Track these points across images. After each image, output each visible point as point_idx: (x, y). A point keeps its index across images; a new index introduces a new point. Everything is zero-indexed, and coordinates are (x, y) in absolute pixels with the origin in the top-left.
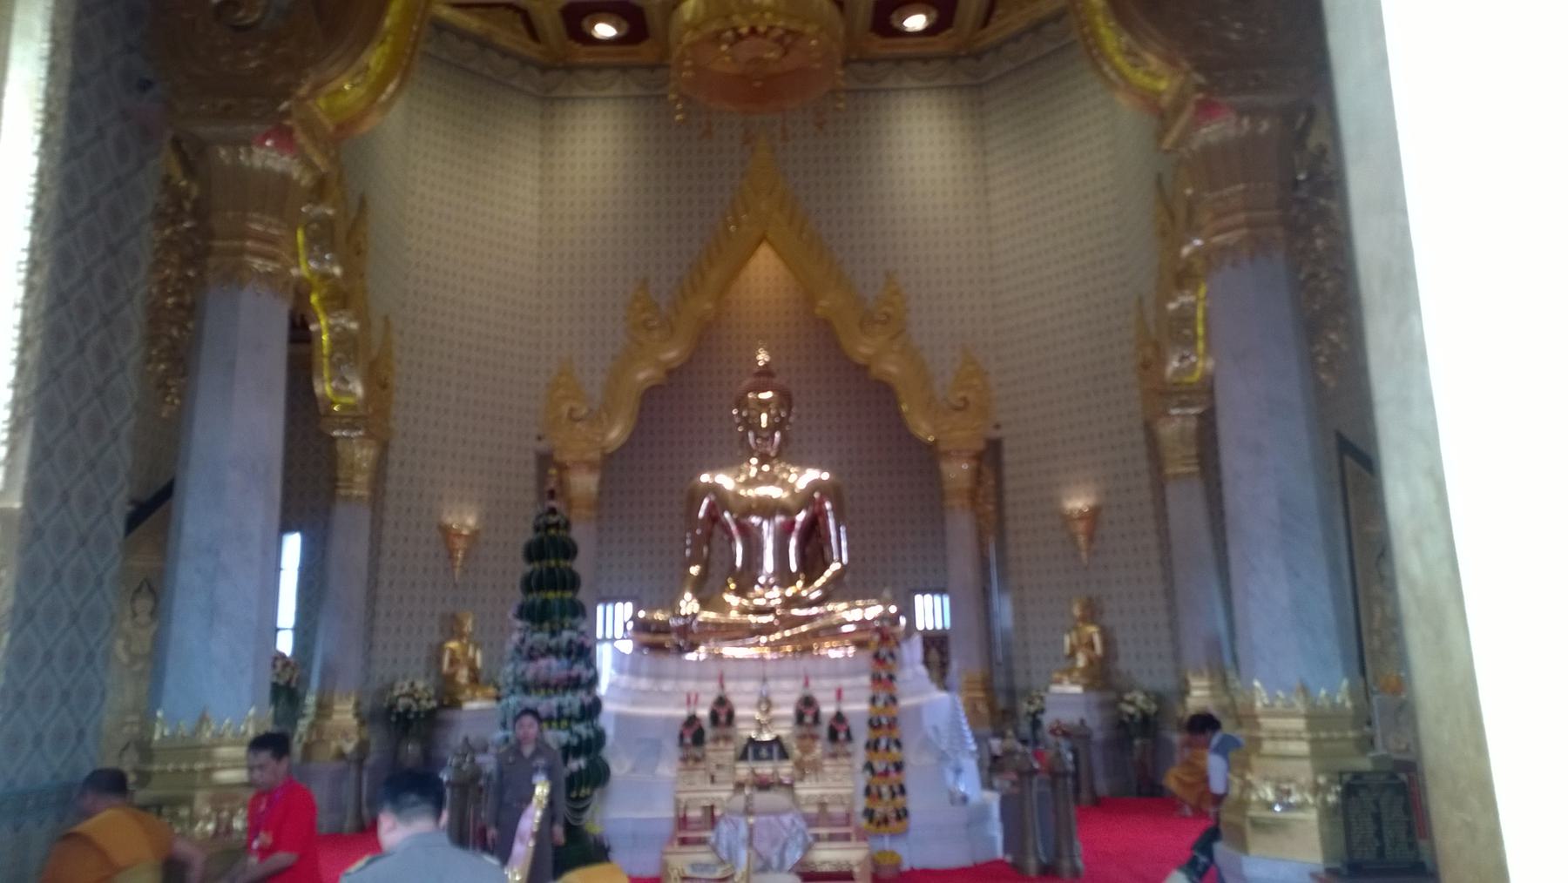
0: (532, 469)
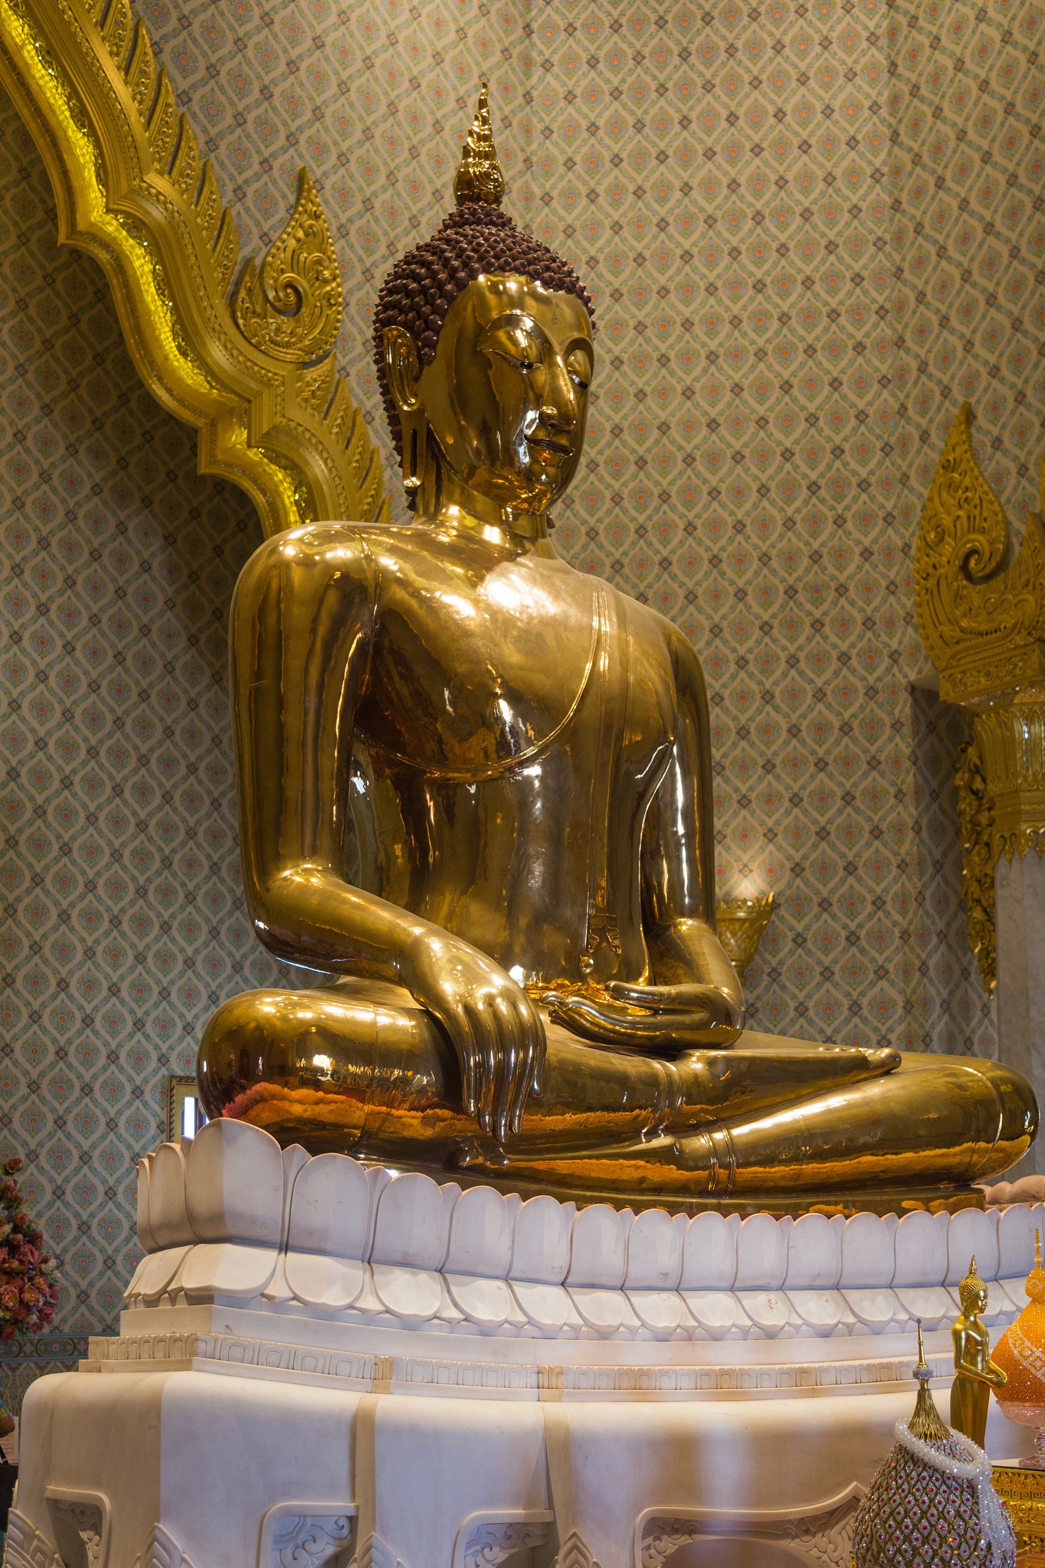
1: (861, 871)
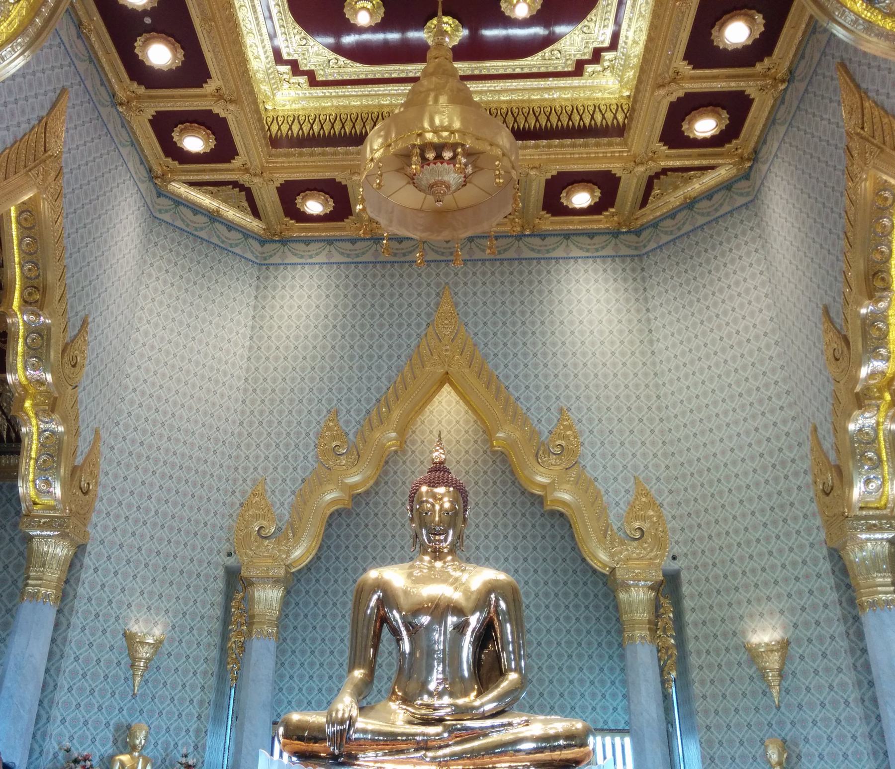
0: (220, 585)
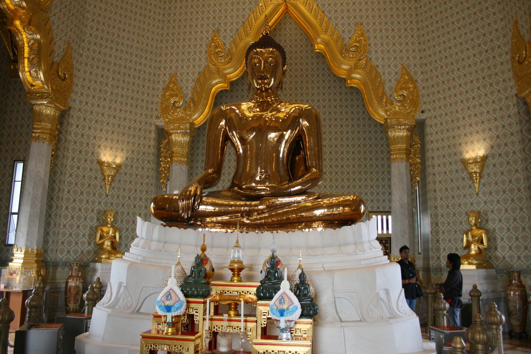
0: (153, 135)
1: (509, 145)
